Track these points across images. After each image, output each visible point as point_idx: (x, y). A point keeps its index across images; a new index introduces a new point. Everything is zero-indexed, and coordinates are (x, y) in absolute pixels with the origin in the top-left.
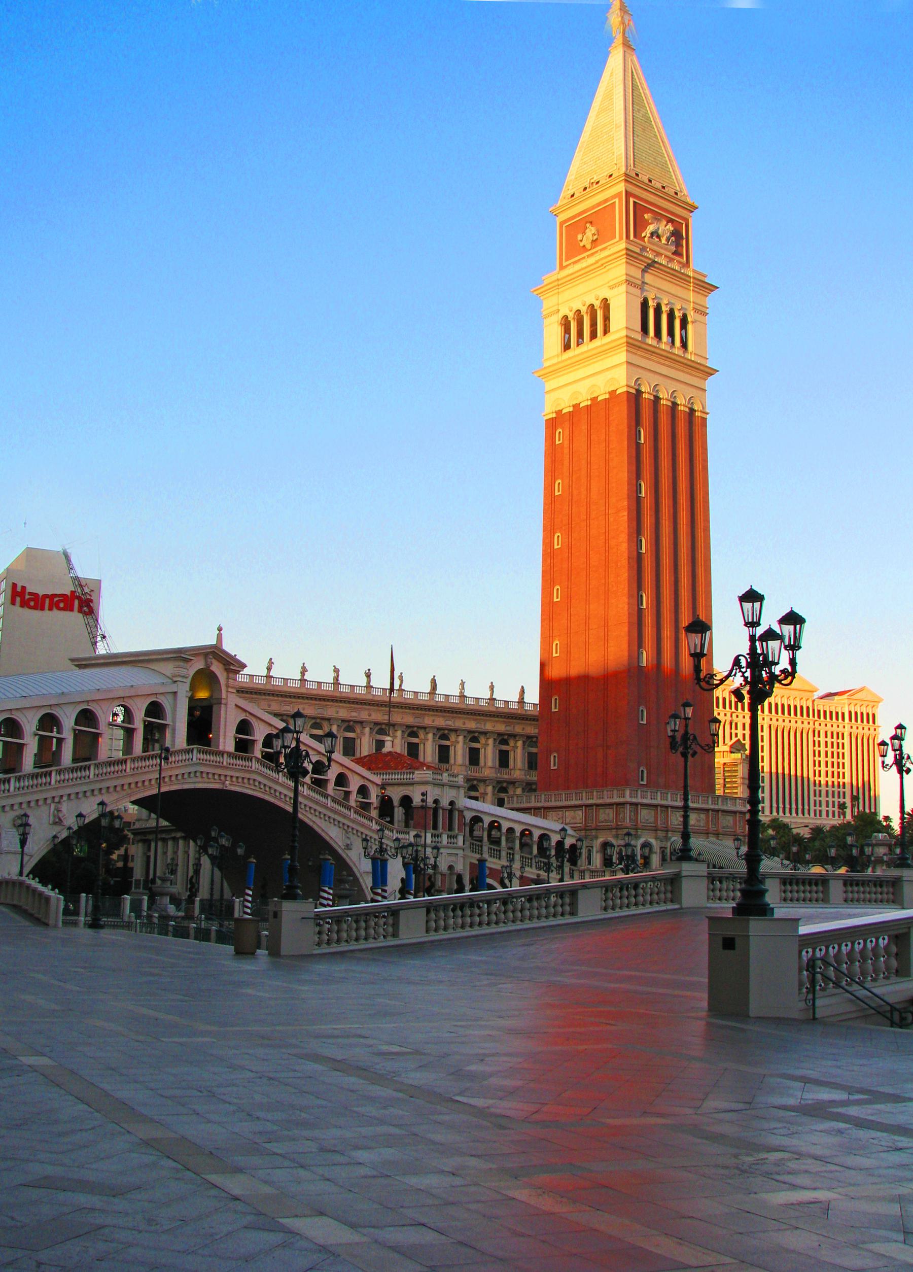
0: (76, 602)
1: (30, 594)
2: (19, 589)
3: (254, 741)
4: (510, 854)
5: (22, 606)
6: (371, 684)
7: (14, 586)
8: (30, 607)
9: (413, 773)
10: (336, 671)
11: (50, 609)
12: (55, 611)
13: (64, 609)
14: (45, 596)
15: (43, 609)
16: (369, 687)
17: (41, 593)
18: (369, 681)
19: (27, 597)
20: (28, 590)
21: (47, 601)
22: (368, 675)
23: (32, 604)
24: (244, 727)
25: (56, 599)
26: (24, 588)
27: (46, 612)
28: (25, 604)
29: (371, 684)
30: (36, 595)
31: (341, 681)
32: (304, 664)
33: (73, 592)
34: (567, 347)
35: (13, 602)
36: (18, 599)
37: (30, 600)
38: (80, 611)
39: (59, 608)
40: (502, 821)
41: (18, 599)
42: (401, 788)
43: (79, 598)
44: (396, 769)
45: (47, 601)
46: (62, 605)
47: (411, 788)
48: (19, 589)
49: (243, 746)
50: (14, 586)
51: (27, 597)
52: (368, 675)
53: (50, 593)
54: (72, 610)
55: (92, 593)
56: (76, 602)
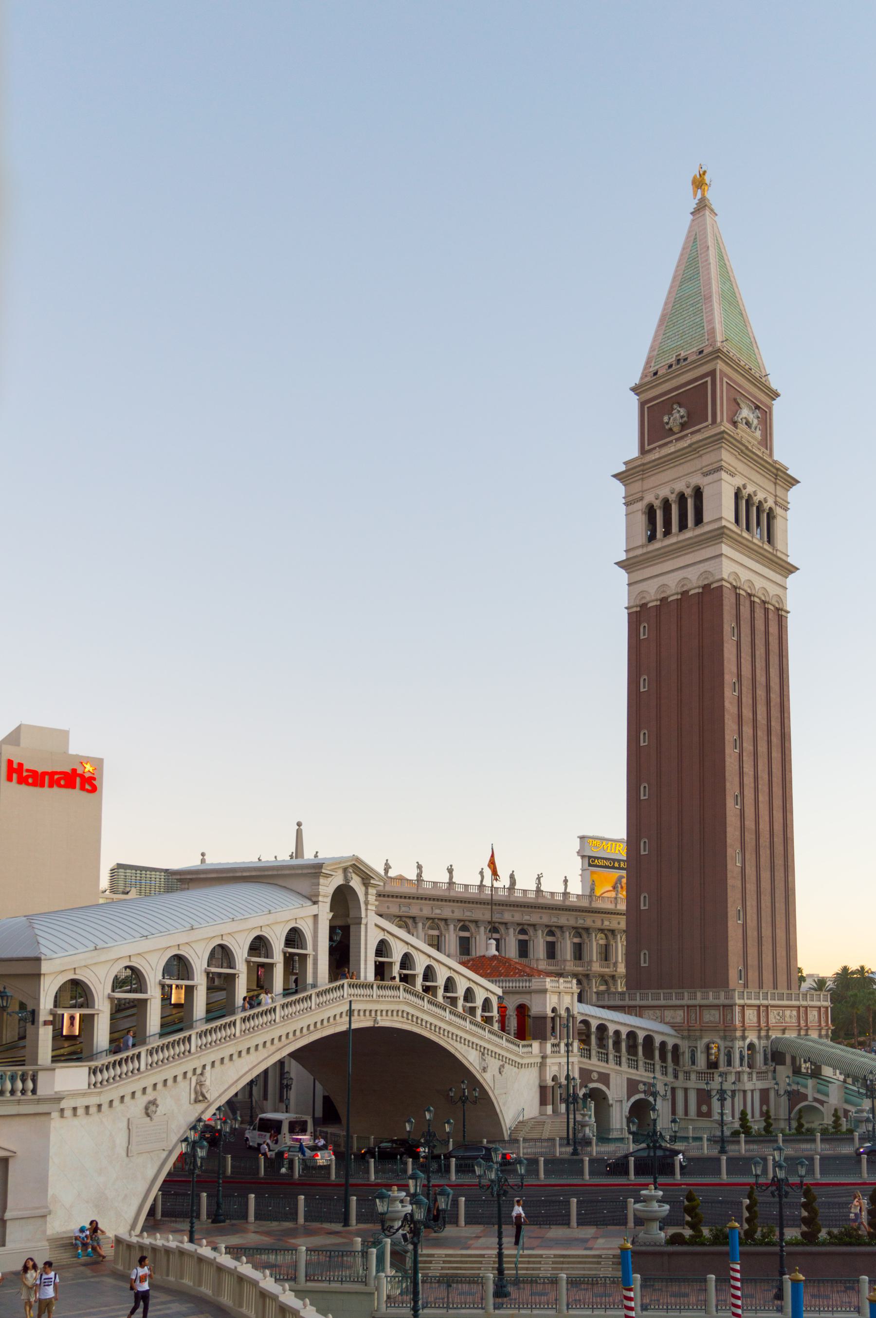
0: (78, 780)
1: (27, 770)
2: (15, 766)
3: (391, 964)
4: (616, 1056)
5: (20, 782)
6: (454, 880)
8: (28, 784)
9: (530, 981)
10: (419, 867)
12: (56, 789)
13: (66, 786)
14: (44, 774)
15: (42, 785)
16: (451, 883)
17: (40, 770)
18: (451, 878)
19: (25, 774)
20: (25, 767)
21: (47, 778)
22: (450, 871)
23: (30, 780)
24: (382, 948)
25: (56, 777)
26: (21, 765)
27: (46, 790)
28: (22, 781)
29: (454, 880)
30: (35, 773)
31: (425, 877)
32: (387, 860)
33: (74, 770)
34: (652, 538)
35: (10, 779)
36: (15, 776)
37: (28, 777)
38: (83, 788)
39: (60, 786)
40: (608, 1024)
41: (15, 776)
42: (518, 996)
43: (82, 776)
44: (508, 976)
45: (47, 778)
47: (528, 996)
48: (15, 766)
49: (381, 970)
50: (10, 762)
51: (25, 774)
52: (450, 871)
53: (50, 770)
54: (74, 787)
56: (78, 780)
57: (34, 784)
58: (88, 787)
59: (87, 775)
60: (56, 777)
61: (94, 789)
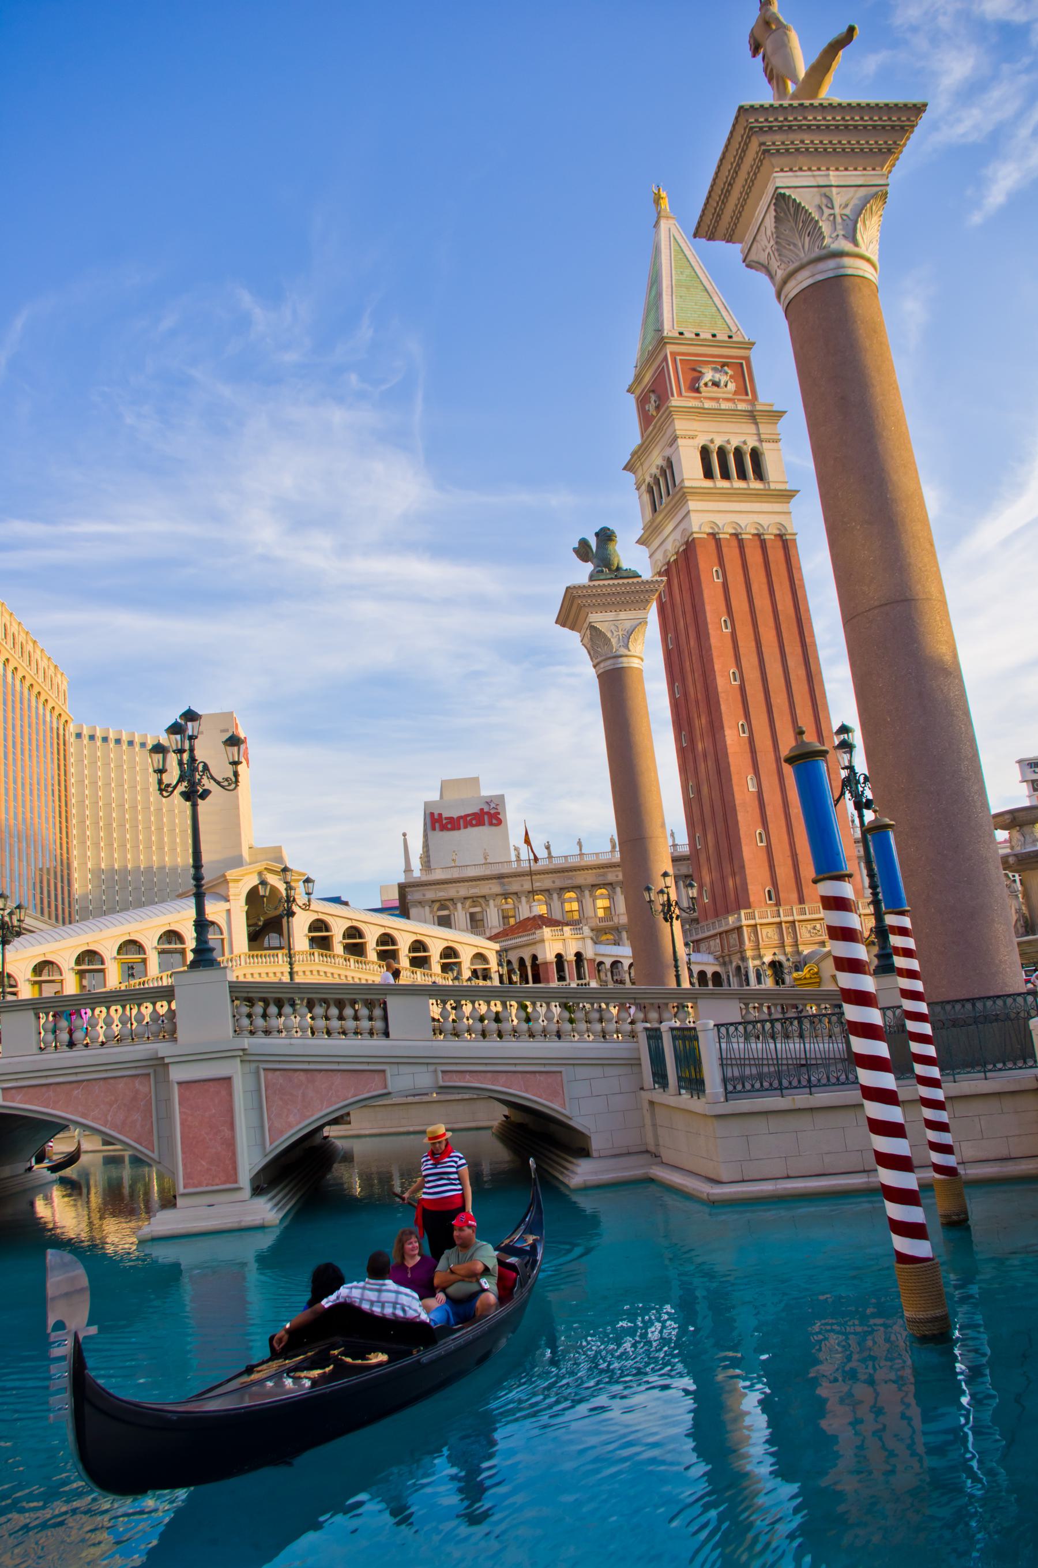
0: (486, 817)
1: (446, 818)
7: (432, 814)
11: (466, 827)
14: (460, 818)
19: (444, 822)
20: (444, 816)
25: (468, 818)
26: (440, 815)
27: (463, 831)
28: (443, 828)
33: (482, 810)
35: (434, 829)
36: (437, 825)
37: (447, 823)
38: (491, 824)
39: (472, 825)
41: (437, 825)
43: (488, 813)
46: (474, 822)
48: (436, 817)
51: (444, 822)
53: (463, 814)
54: (484, 824)
55: (498, 807)
56: (486, 817)
57: (453, 829)
58: (494, 821)
59: (492, 812)
60: (468, 818)
61: (500, 822)
